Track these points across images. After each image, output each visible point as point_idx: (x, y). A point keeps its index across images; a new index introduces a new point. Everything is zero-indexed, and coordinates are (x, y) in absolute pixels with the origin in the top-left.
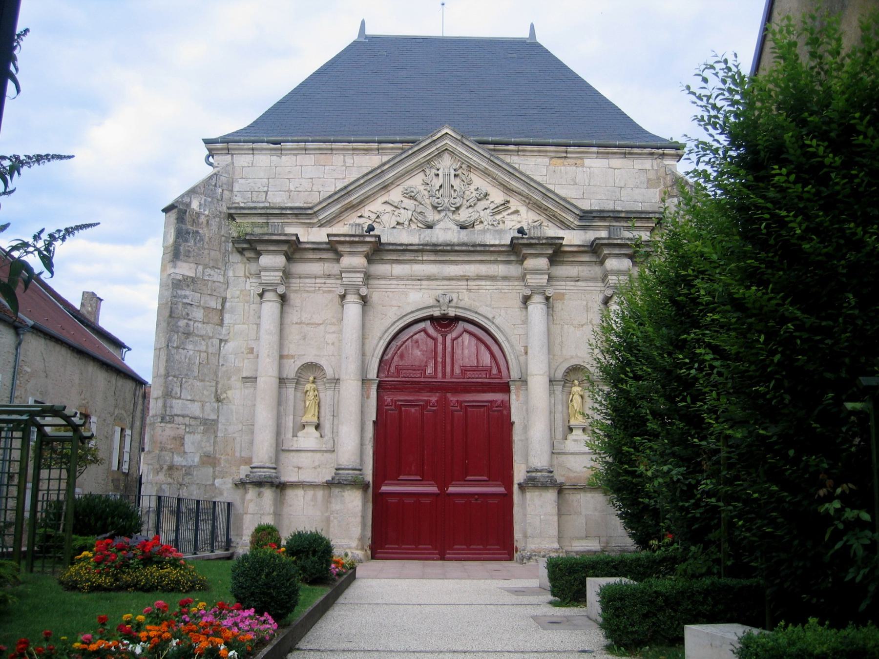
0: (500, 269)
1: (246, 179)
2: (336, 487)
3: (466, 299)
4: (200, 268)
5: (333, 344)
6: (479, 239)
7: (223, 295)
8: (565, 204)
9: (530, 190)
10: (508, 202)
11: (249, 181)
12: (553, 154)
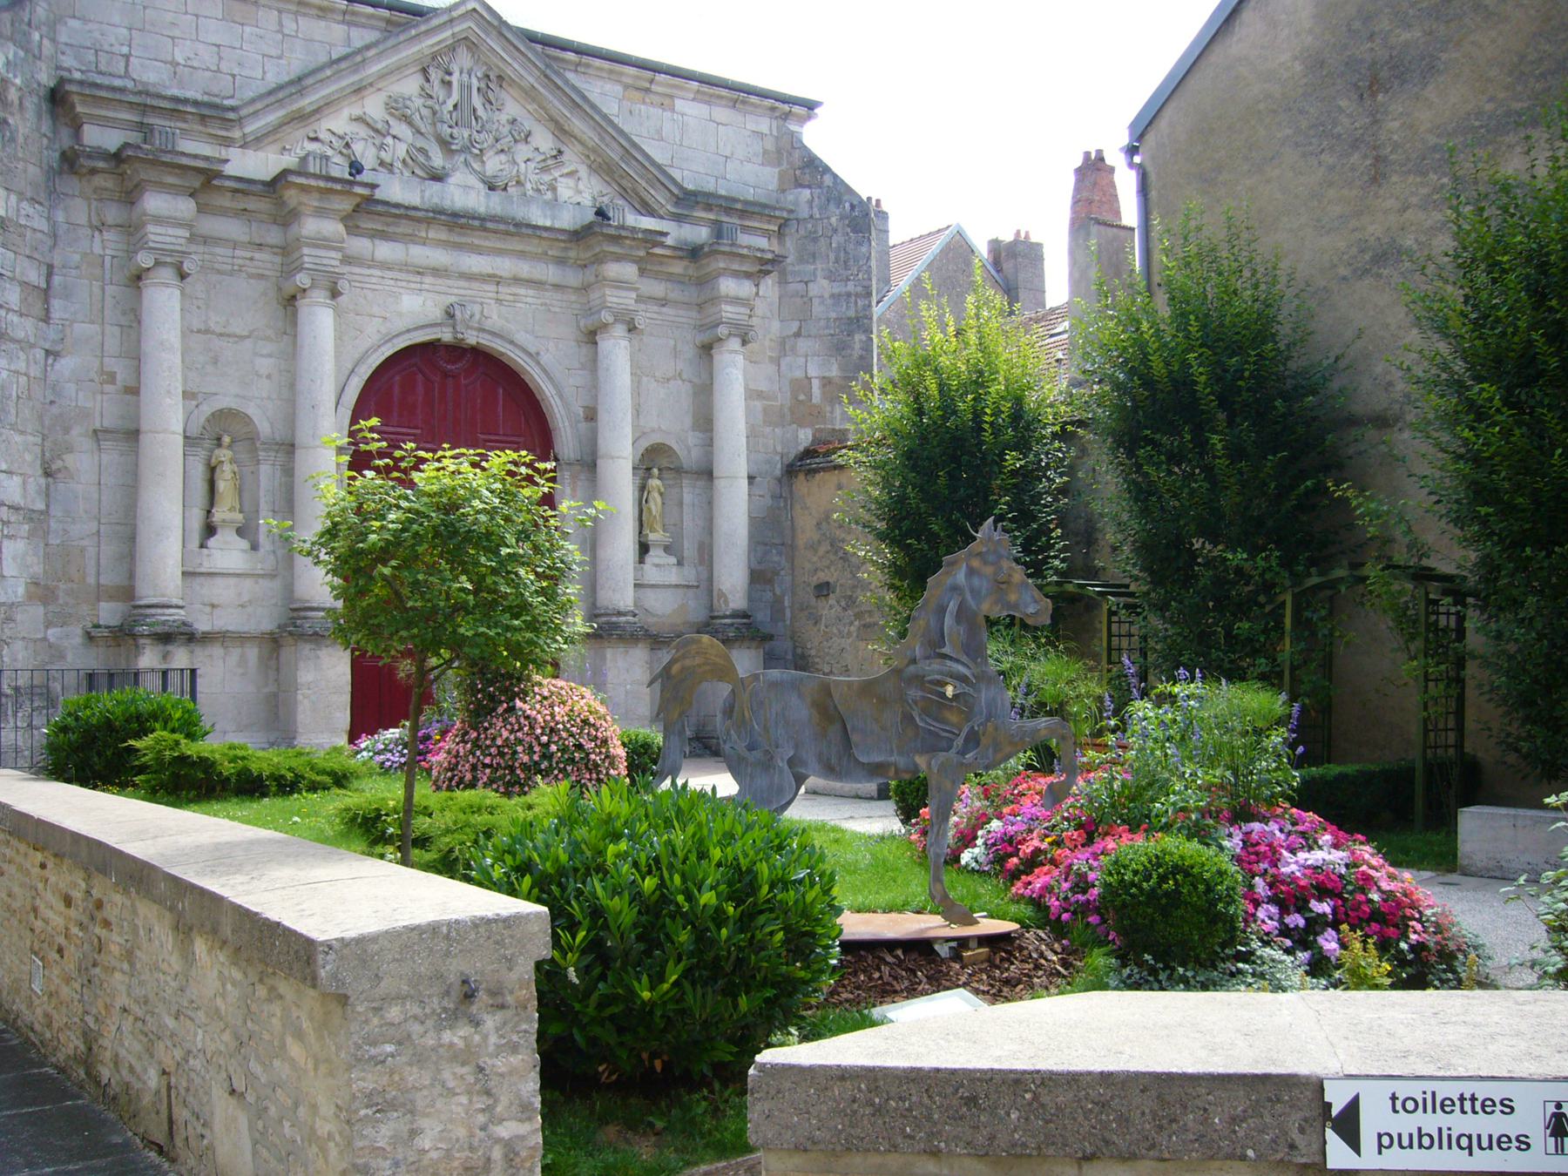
0: (550, 273)
1: (85, 20)
2: (306, 641)
3: (495, 317)
4: (13, 198)
5: (269, 377)
6: (520, 212)
7: (48, 260)
8: (659, 175)
9: (602, 139)
10: (560, 152)
11: (90, 26)
12: (630, 81)
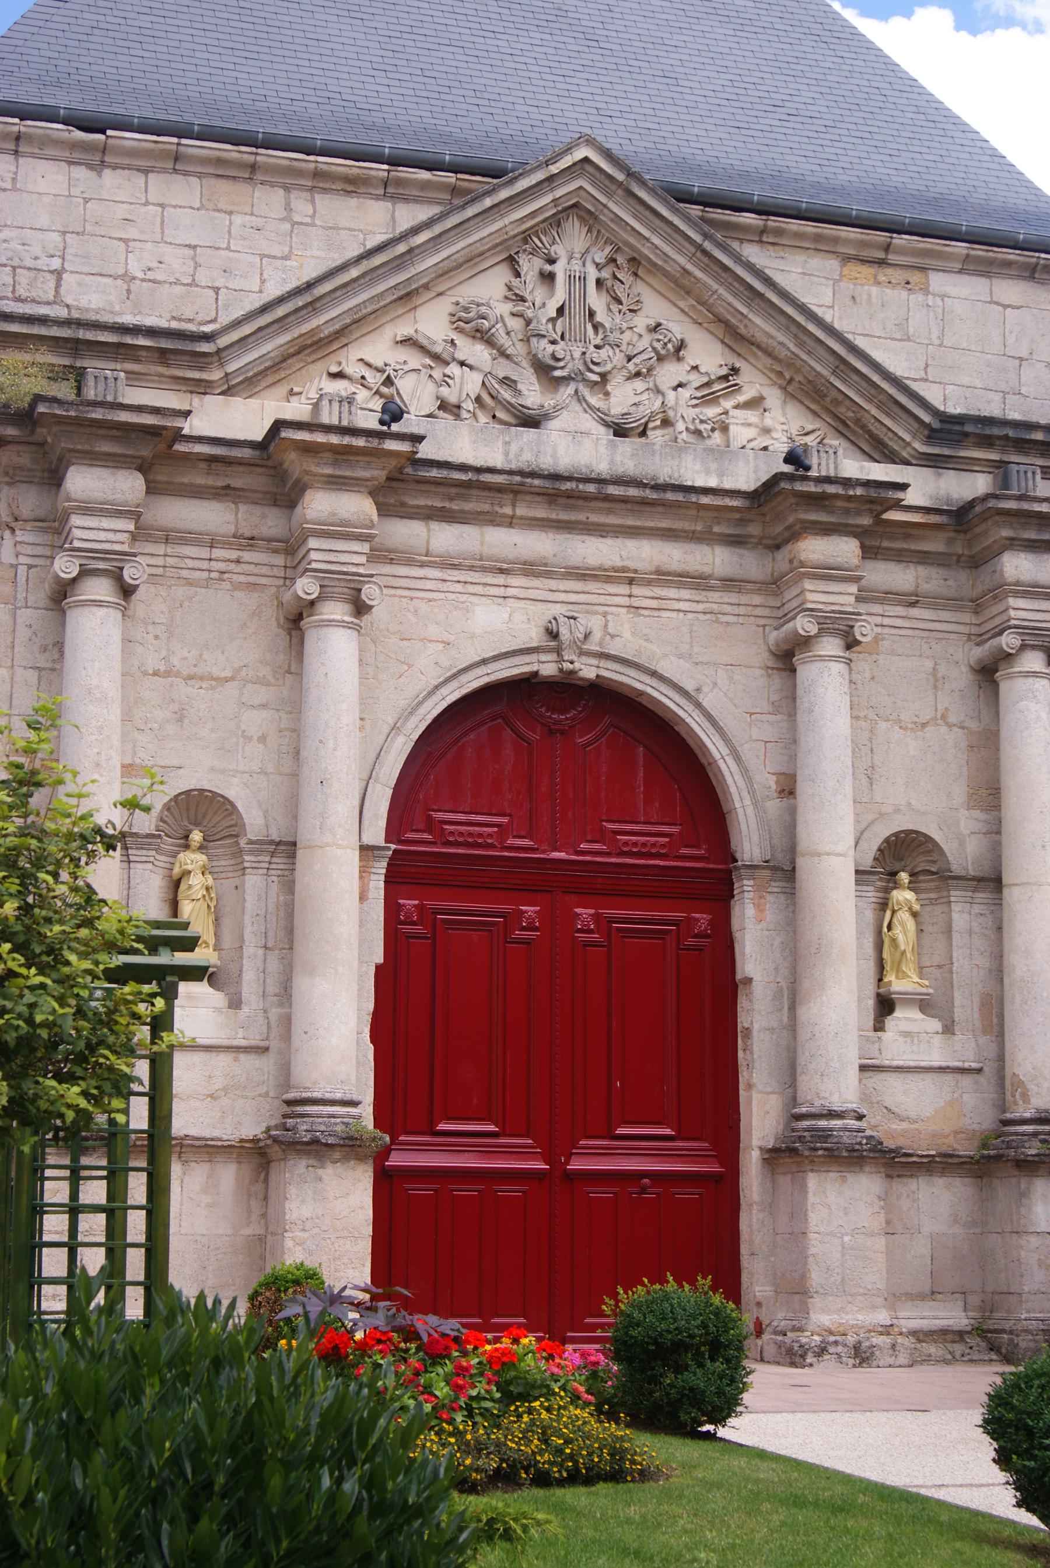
0: (717, 559)
3: (627, 634)
5: (262, 739)
8: (896, 395)
9: (801, 345)
10: (735, 371)
